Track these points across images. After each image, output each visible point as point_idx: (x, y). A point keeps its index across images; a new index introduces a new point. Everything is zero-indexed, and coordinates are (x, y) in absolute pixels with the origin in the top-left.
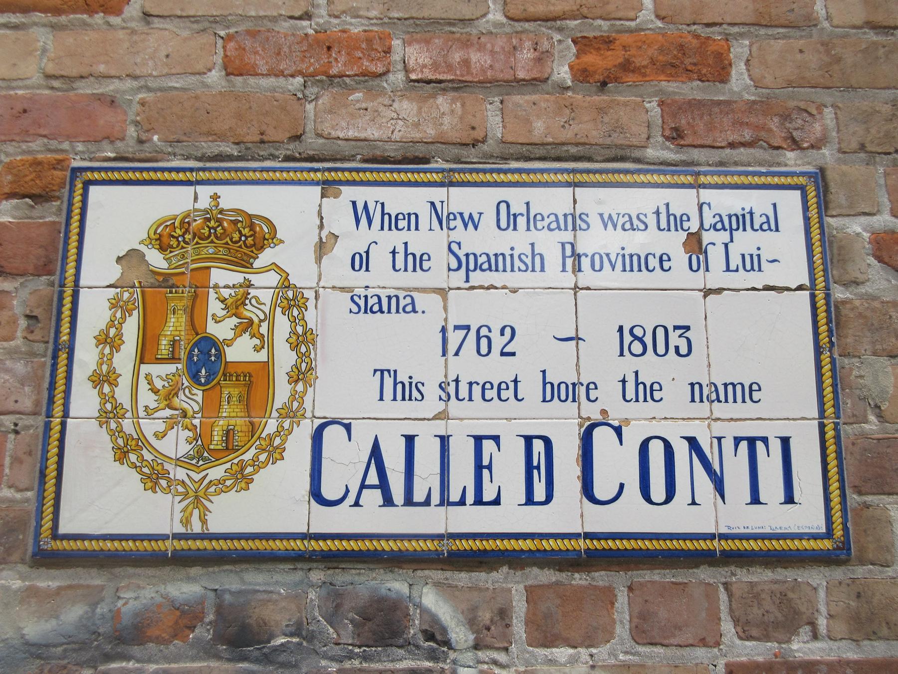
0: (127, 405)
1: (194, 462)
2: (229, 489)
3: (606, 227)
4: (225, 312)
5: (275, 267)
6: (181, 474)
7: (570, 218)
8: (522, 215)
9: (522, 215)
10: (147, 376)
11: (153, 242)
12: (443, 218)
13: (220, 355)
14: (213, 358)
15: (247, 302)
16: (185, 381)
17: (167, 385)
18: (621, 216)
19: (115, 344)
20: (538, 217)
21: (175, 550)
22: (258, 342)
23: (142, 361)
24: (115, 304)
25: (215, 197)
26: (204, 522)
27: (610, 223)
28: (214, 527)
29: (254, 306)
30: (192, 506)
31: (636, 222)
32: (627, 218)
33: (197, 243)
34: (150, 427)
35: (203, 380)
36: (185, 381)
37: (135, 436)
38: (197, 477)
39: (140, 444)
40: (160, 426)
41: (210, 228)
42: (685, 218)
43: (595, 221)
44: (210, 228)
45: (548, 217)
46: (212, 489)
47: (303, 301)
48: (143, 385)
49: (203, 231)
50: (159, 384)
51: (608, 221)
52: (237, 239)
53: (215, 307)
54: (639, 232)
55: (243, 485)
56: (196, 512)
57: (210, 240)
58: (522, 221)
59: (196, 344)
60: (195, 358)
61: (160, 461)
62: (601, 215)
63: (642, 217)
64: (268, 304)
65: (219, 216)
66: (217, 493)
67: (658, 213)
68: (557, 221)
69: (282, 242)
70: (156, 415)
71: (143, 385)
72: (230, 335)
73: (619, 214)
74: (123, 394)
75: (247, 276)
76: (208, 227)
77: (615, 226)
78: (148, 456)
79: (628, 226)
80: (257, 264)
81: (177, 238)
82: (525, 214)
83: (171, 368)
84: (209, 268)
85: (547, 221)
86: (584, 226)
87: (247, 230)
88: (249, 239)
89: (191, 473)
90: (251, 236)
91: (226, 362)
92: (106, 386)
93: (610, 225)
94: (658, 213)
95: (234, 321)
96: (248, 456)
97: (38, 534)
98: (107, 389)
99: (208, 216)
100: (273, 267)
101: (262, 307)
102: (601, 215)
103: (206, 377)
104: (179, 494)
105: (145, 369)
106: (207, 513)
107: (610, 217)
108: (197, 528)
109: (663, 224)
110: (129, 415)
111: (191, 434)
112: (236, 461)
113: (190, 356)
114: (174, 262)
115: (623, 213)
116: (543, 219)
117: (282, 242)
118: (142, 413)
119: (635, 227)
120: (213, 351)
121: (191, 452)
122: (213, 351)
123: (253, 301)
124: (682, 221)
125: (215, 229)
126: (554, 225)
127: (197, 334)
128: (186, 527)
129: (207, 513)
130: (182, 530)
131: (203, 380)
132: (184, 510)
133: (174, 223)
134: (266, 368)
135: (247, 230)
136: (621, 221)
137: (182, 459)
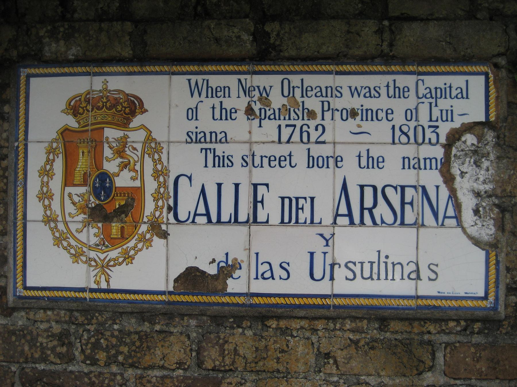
0: (58, 212)
1: (100, 247)
2: (120, 264)
3: (353, 96)
4: (112, 156)
5: (143, 127)
6: (93, 254)
7: (329, 90)
8: (299, 88)
9: (299, 88)
10: (70, 195)
11: (69, 111)
12: (247, 92)
13: (112, 182)
14: (108, 185)
15: (127, 149)
16: (91, 198)
17: (81, 200)
18: (363, 88)
19: (50, 175)
20: (309, 89)
21: (90, 298)
22: (133, 174)
23: (66, 185)
24: (49, 153)
25: (106, 82)
26: (108, 282)
27: (356, 92)
28: (114, 286)
29: (131, 151)
30: (101, 273)
31: (373, 92)
32: (367, 89)
33: (96, 112)
34: (73, 227)
35: (102, 198)
36: (91, 198)
37: (65, 231)
38: (102, 256)
39: (68, 236)
40: (80, 226)
41: (103, 103)
42: (406, 89)
43: (346, 92)
44: (103, 103)
45: (315, 89)
46: (112, 263)
47: (160, 148)
48: (67, 201)
49: (99, 104)
50: (76, 199)
51: (354, 91)
52: (120, 109)
53: (108, 152)
54: (375, 98)
55: (129, 260)
56: (103, 277)
57: (103, 110)
58: (298, 93)
59: (98, 176)
60: (97, 185)
61: (80, 246)
62: (350, 87)
63: (377, 89)
64: (140, 150)
65: (108, 94)
66: (114, 266)
67: (388, 86)
68: (321, 91)
69: (146, 111)
70: (77, 219)
71: (67, 201)
72: (116, 170)
73: (362, 87)
74: (56, 205)
75: (126, 133)
76: (102, 102)
77: (359, 96)
78: (73, 243)
79: (368, 95)
80: (132, 125)
81: (83, 108)
82: (300, 86)
83: (83, 190)
84: (103, 128)
85: (315, 91)
86: (339, 95)
87: (126, 103)
88: (127, 109)
89: (97, 253)
90: (127, 108)
91: (116, 187)
92: (46, 200)
93: (356, 94)
94: (388, 86)
95: (119, 160)
96: (131, 244)
97: (15, 288)
98: (47, 202)
99: (101, 94)
100: (142, 126)
101: (135, 152)
102: (350, 87)
103: (104, 196)
104: (90, 265)
105: (68, 190)
106: (110, 277)
107: (356, 88)
108: (104, 285)
109: (391, 93)
110: (60, 219)
111: (96, 230)
112: (125, 247)
113: (94, 183)
114: (82, 123)
115: (365, 86)
116: (312, 90)
117: (146, 111)
118: (68, 219)
119: (372, 95)
120: (108, 180)
121: (98, 242)
122: (108, 180)
123: (130, 148)
124: (404, 92)
125: (106, 103)
126: (319, 94)
127: (98, 170)
128: (98, 284)
129: (110, 277)
130: (94, 286)
131: (102, 198)
132: (96, 275)
133: (80, 100)
134: (140, 190)
135: (126, 103)
136: (364, 91)
137: (92, 246)
